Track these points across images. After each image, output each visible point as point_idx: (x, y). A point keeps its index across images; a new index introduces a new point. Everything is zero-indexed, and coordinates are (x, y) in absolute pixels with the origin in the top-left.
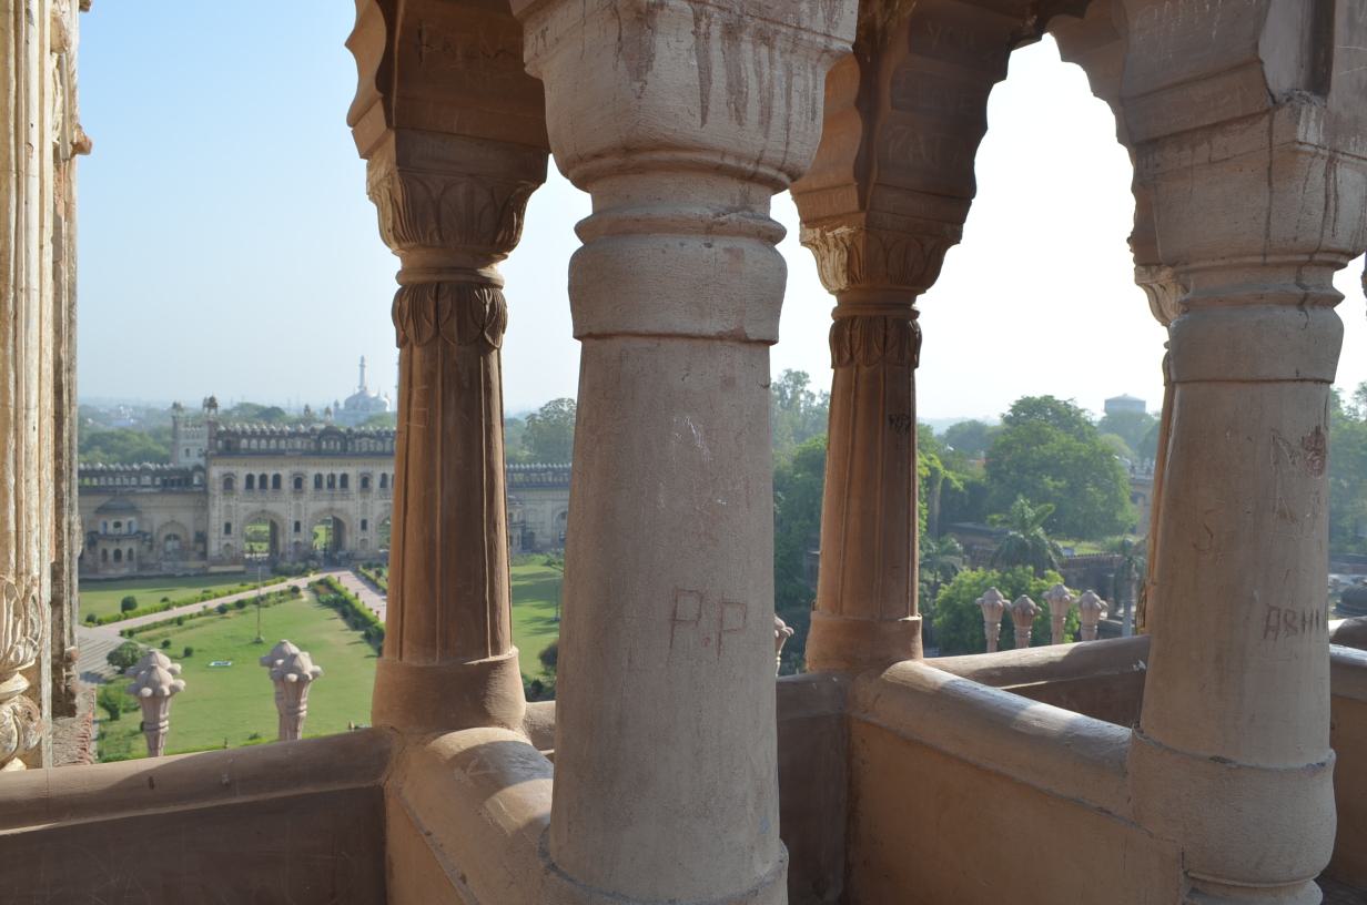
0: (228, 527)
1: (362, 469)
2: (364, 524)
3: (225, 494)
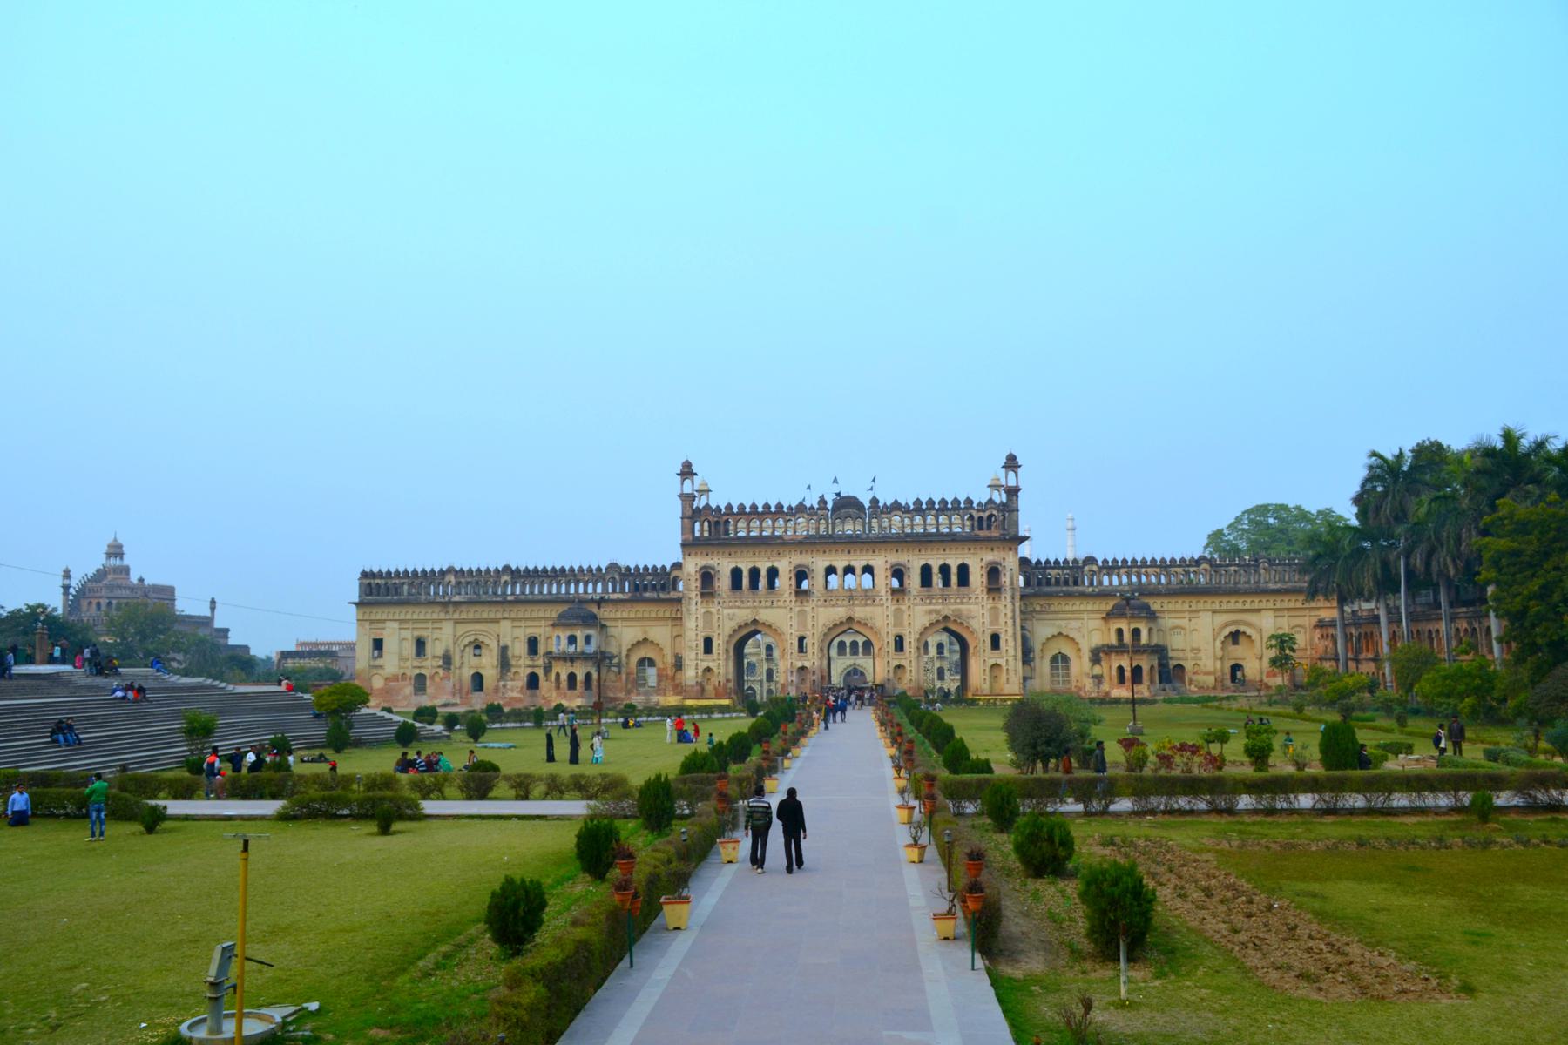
2: (899, 643)
3: (703, 595)
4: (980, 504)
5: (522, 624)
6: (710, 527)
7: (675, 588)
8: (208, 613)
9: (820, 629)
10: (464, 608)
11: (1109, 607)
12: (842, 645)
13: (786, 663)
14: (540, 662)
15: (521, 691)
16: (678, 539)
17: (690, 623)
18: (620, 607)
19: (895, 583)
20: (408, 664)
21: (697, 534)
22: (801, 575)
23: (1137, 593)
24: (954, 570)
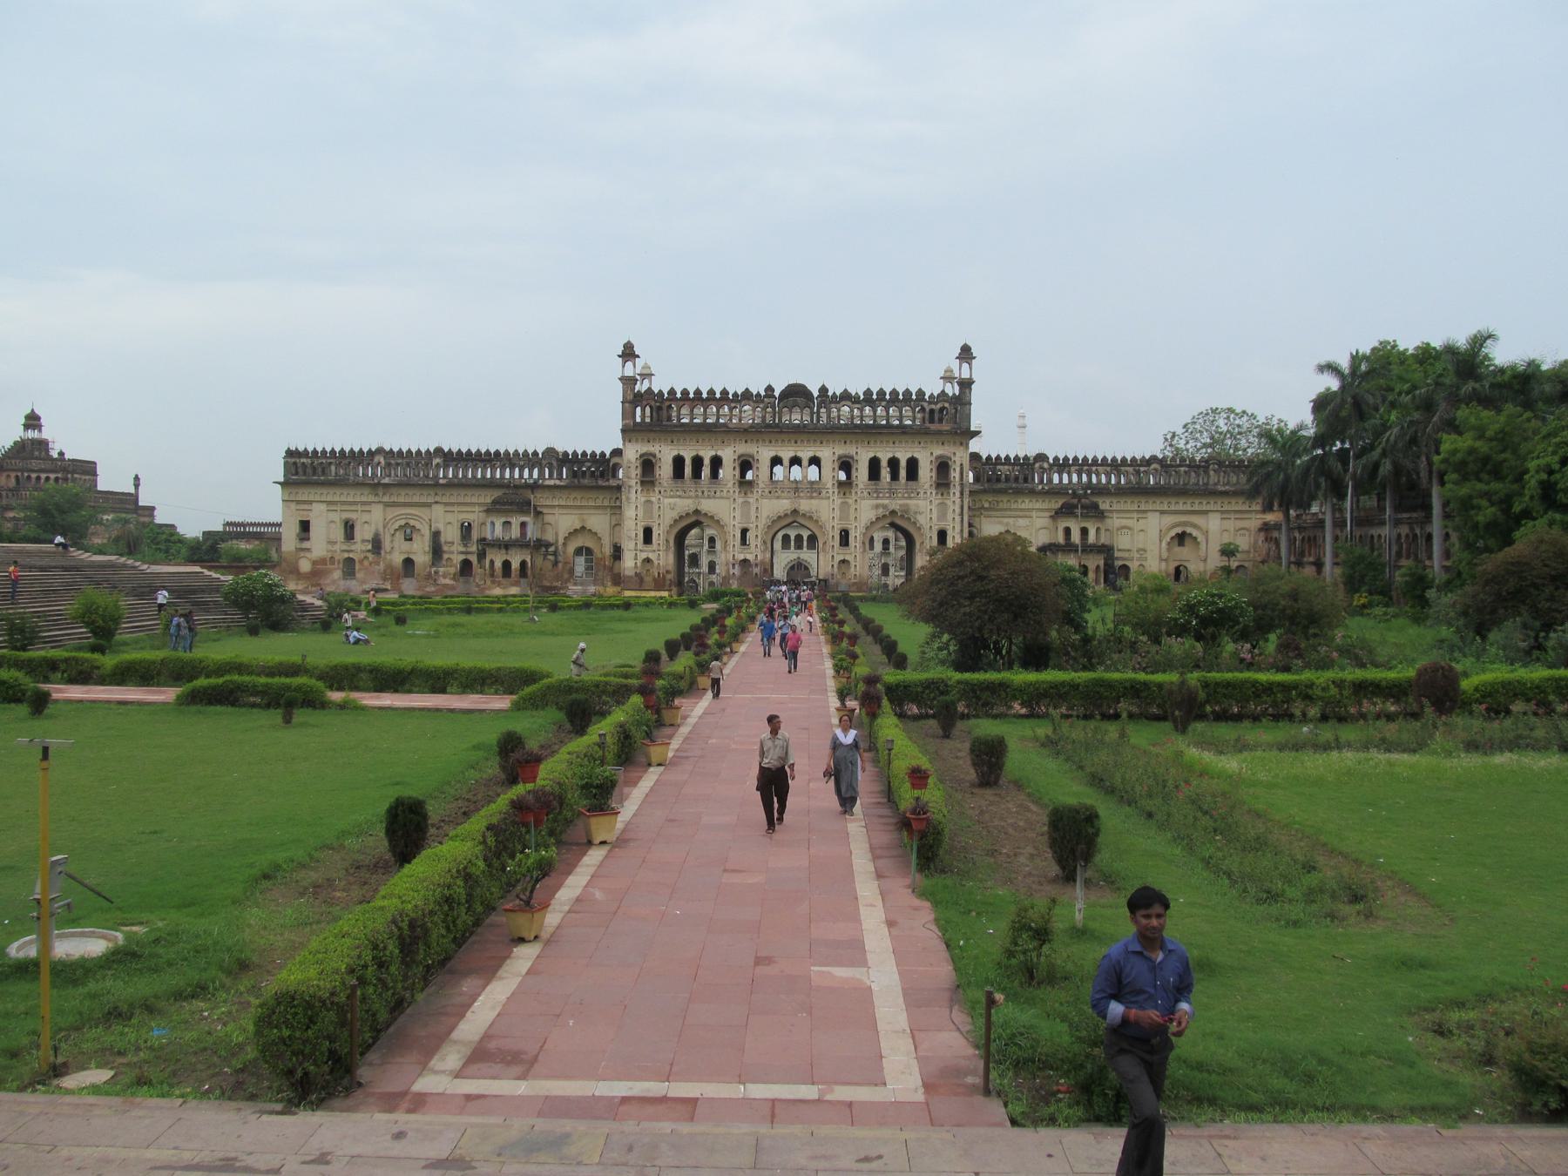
0: (648, 533)
1: (841, 450)
2: (845, 538)
3: (643, 483)
4: (932, 396)
5: (455, 508)
6: (652, 412)
7: (615, 475)
8: (132, 491)
9: (763, 522)
10: (394, 490)
11: (1058, 505)
12: (786, 538)
13: (728, 555)
14: (474, 549)
15: (454, 579)
16: (617, 423)
17: (630, 512)
18: (557, 493)
19: (842, 476)
20: (337, 547)
21: (638, 420)
22: (745, 465)
23: (1086, 490)
24: (903, 464)
